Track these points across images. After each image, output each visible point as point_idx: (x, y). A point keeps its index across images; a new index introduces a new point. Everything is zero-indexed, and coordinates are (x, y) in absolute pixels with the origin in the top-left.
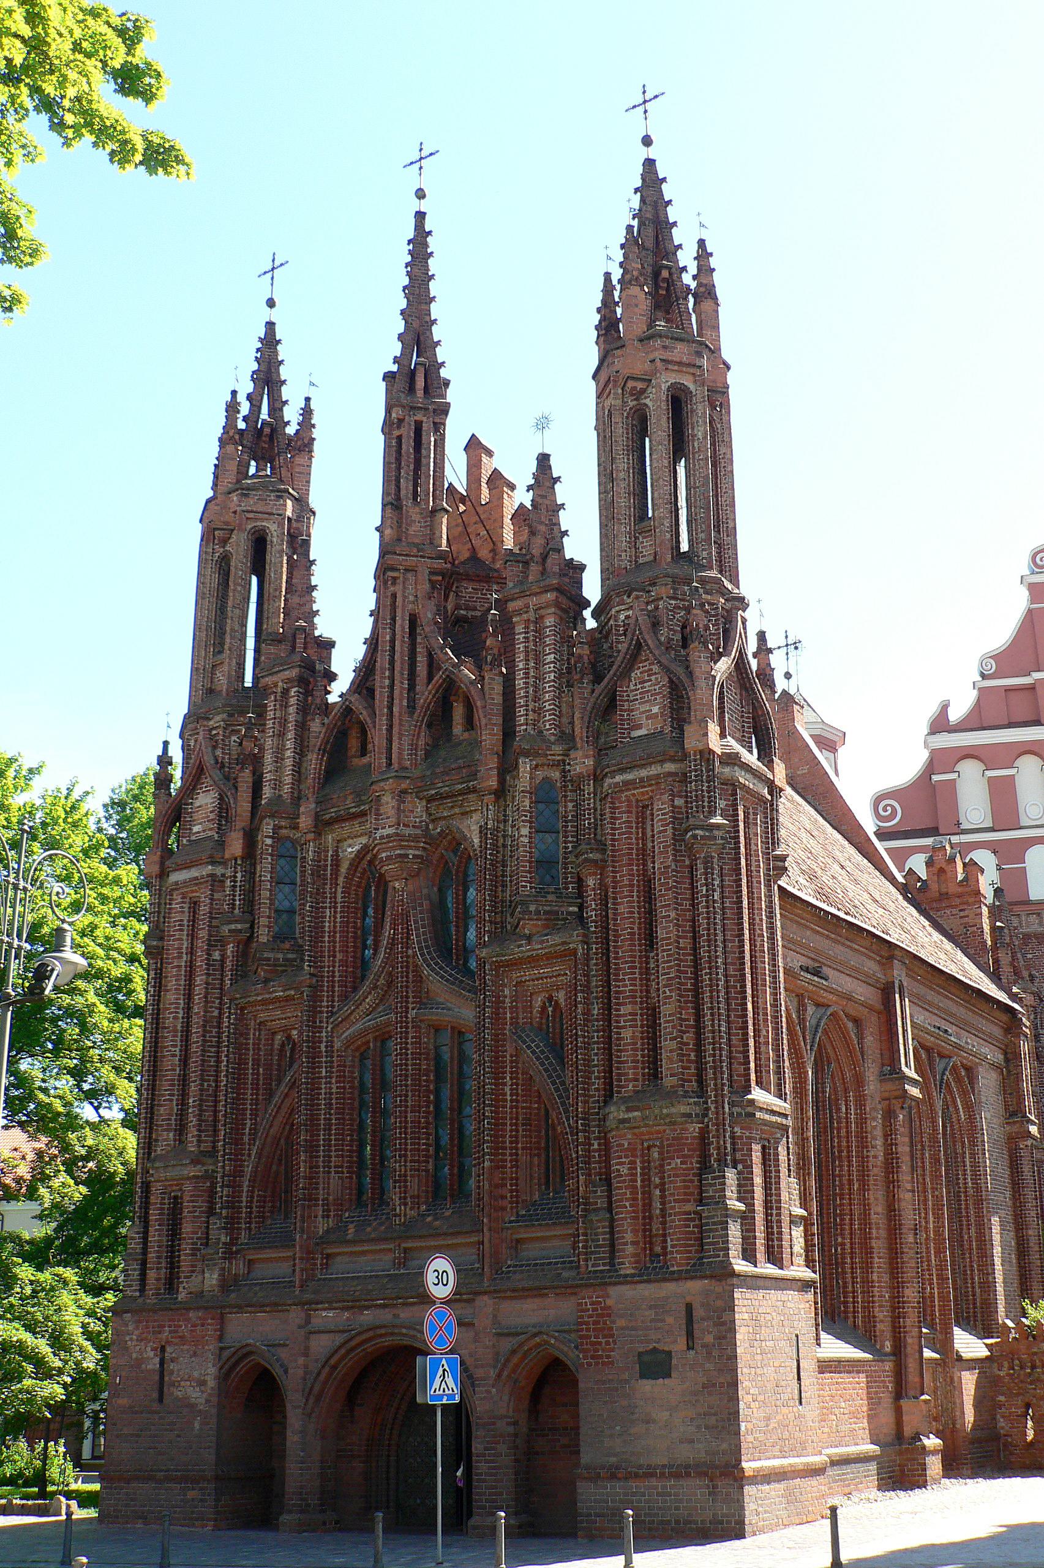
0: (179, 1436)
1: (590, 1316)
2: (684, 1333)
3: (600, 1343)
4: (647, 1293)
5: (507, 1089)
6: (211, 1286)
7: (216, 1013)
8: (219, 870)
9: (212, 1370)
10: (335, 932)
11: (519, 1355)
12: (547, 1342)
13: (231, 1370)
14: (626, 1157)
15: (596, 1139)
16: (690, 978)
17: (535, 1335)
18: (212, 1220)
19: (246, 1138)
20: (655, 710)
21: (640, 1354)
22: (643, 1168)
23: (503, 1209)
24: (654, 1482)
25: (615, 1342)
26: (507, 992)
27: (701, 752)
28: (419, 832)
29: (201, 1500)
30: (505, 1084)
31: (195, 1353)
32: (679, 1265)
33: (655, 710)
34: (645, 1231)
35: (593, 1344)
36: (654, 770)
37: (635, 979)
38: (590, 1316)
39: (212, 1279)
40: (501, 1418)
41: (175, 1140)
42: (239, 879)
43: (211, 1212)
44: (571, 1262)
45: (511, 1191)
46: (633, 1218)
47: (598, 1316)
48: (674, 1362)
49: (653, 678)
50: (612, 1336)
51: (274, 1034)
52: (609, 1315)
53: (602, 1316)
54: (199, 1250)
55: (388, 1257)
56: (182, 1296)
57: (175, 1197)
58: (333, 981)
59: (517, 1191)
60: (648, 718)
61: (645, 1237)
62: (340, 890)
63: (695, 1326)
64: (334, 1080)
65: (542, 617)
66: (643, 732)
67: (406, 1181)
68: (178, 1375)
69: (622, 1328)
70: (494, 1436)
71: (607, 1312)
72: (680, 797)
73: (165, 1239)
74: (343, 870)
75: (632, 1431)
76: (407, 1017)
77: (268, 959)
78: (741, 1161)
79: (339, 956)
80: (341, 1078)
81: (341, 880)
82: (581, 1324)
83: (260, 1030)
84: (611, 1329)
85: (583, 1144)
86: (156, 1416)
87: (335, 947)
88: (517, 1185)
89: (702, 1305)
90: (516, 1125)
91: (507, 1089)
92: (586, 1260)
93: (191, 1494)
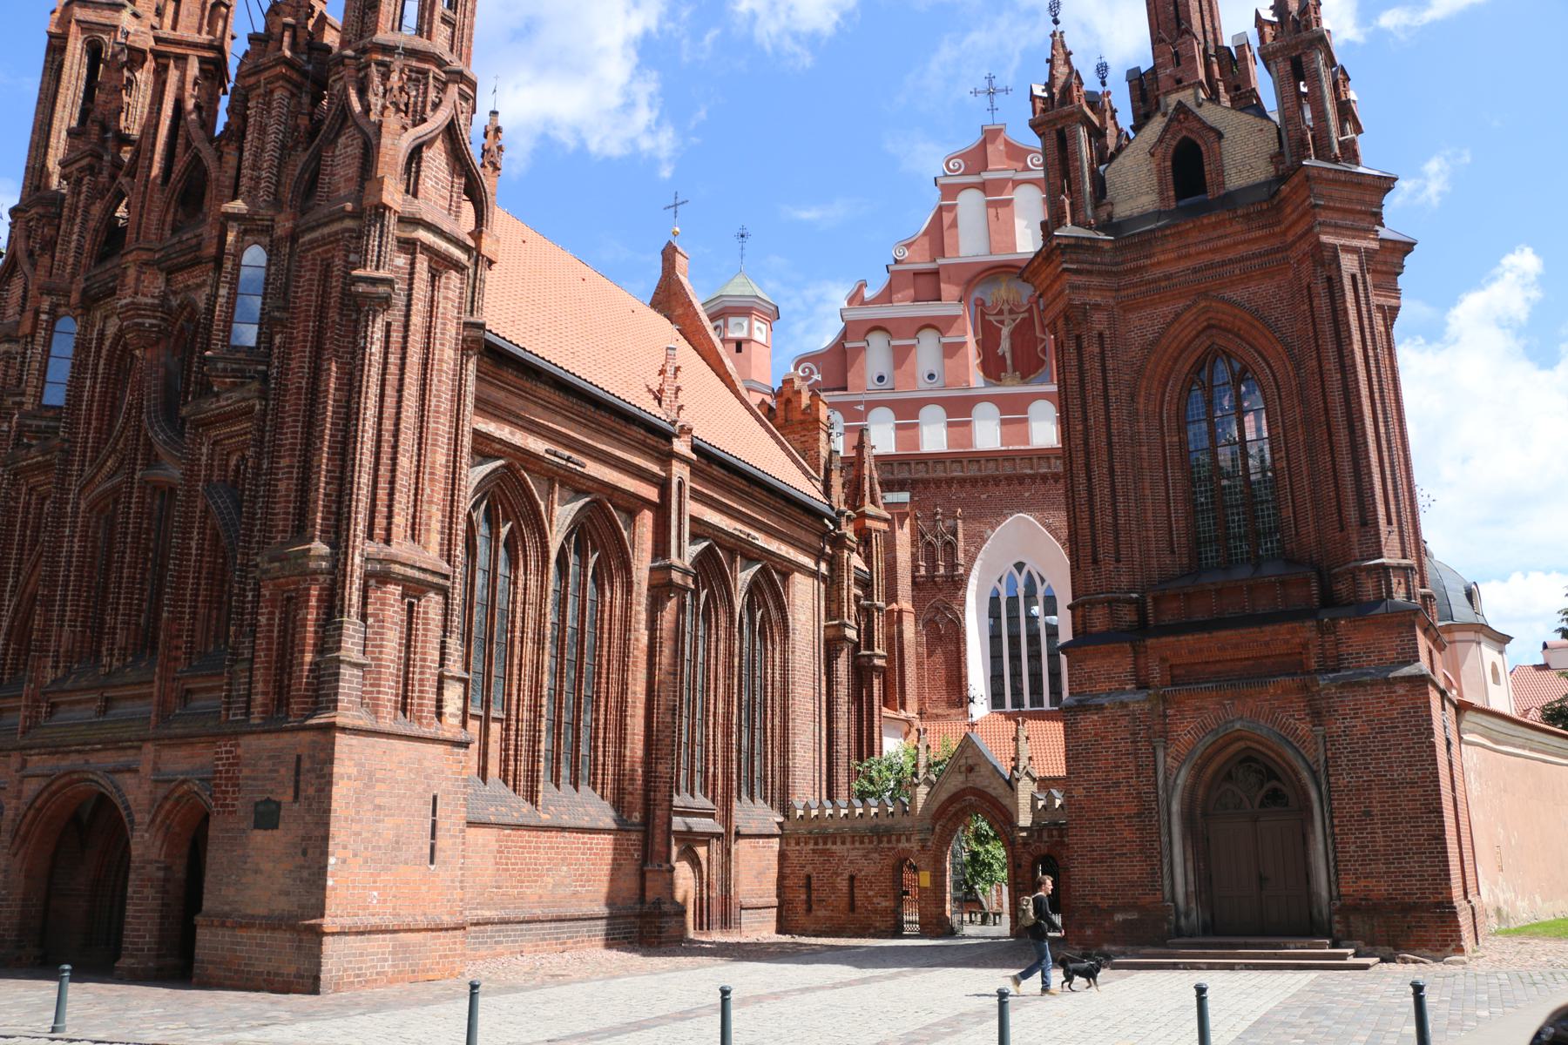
2: (292, 784)
3: (228, 792)
5: (193, 544)
10: (92, 401)
15: (251, 590)
16: (341, 430)
21: (257, 804)
23: (177, 659)
24: (254, 933)
26: (204, 450)
27: (377, 207)
28: (156, 301)
30: (192, 539)
37: (296, 432)
38: (224, 765)
40: (151, 862)
45: (186, 642)
46: (266, 668)
48: (282, 813)
50: (238, 785)
51: (44, 499)
52: (237, 764)
58: (86, 447)
59: (192, 642)
61: (275, 687)
62: (102, 362)
63: (302, 777)
64: (76, 540)
65: (272, 92)
67: (115, 634)
69: (247, 778)
70: (142, 880)
71: (236, 762)
72: (356, 253)
74: (107, 343)
76: (133, 478)
77: (30, 426)
78: (372, 615)
79: (94, 423)
80: (84, 538)
81: (104, 353)
82: (216, 772)
83: (30, 495)
85: (237, 595)
87: (90, 415)
88: (192, 636)
89: (309, 756)
90: (198, 578)
91: (193, 544)
92: (228, 710)
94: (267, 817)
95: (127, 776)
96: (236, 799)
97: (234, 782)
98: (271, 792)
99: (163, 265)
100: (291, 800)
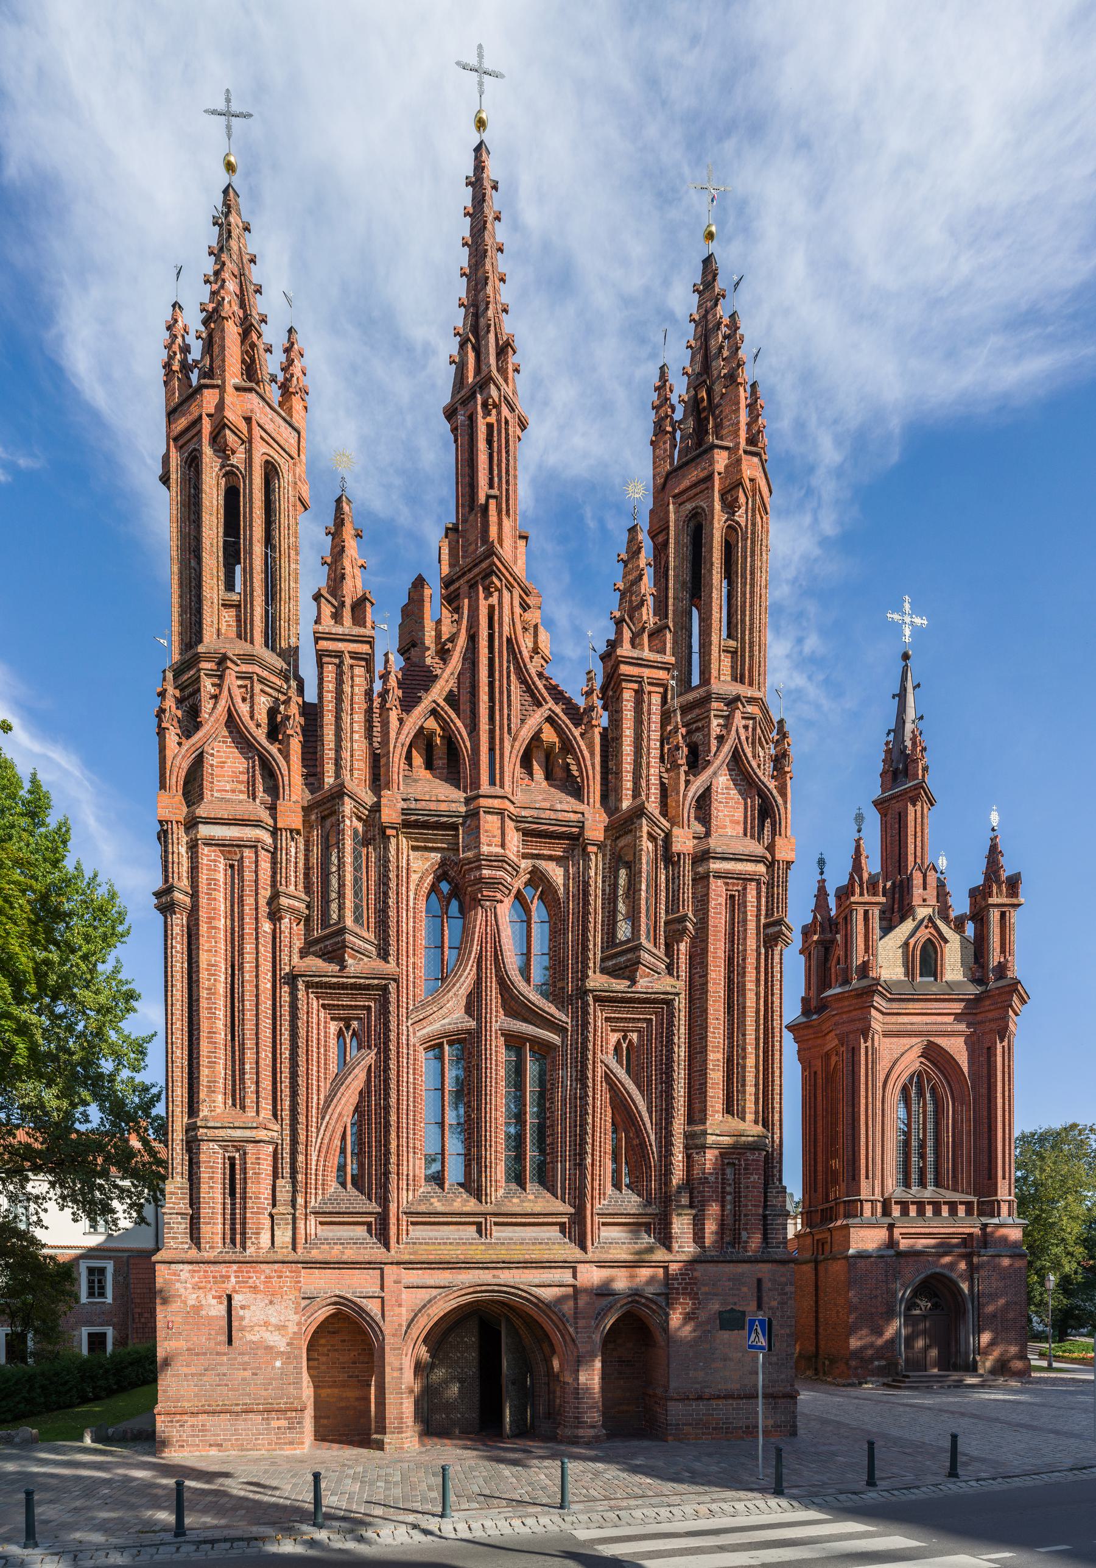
0: (254, 1374)
4: (727, 1270)
12: (637, 1302)
18: (280, 1182)
22: (723, 1179)
29: (289, 1428)
31: (271, 1302)
47: (686, 1284)
52: (695, 1284)
53: (690, 1284)
54: (266, 1209)
56: (251, 1250)
57: (229, 1158)
69: (706, 1294)
84: (697, 1294)
86: (225, 1358)
93: (275, 1424)
98: (735, 1304)
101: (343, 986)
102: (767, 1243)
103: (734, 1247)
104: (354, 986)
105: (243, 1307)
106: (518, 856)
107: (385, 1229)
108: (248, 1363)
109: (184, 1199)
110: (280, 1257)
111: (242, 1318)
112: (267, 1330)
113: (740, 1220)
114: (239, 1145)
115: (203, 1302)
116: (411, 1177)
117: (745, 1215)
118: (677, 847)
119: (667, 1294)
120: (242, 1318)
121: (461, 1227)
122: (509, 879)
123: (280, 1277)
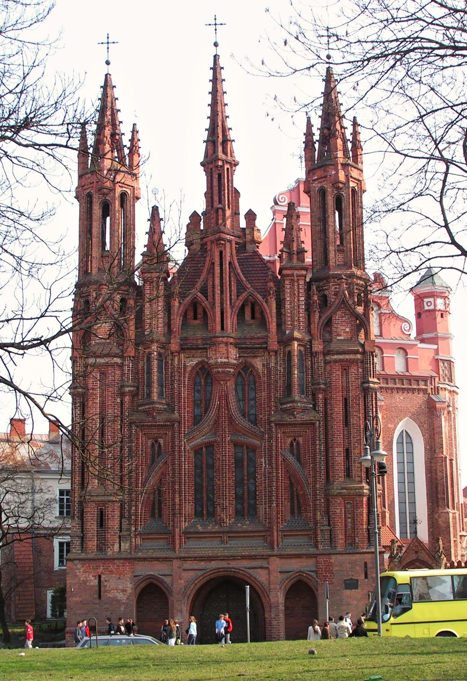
1: (323, 566)
5: (280, 475)
6: (125, 549)
7: (119, 427)
8: (118, 360)
9: (130, 585)
11: (288, 580)
12: (302, 576)
13: (138, 586)
14: (339, 506)
17: (297, 572)
19: (140, 485)
20: (348, 330)
21: (345, 580)
25: (334, 576)
31: (119, 578)
32: (361, 548)
33: (348, 330)
34: (346, 534)
35: (324, 576)
36: (352, 357)
38: (323, 566)
39: (125, 546)
41: (98, 483)
42: (131, 366)
43: (122, 516)
44: (311, 545)
48: (359, 583)
49: (347, 316)
51: (149, 439)
52: (331, 566)
53: (329, 566)
55: (219, 539)
56: (110, 553)
60: (344, 332)
61: (346, 537)
66: (342, 338)
68: (110, 587)
69: (337, 570)
71: (331, 564)
73: (96, 527)
75: (342, 608)
77: (158, 408)
81: (187, 375)
94: (351, 584)
95: (259, 570)
96: (333, 578)
97: (331, 572)
99: (238, 346)
100: (364, 578)
101: (154, 426)
102: (370, 543)
103: (352, 546)
104: (158, 425)
105: (106, 581)
106: (236, 359)
107: (174, 541)
108: (109, 608)
109: (79, 529)
110: (123, 556)
111: (106, 586)
112: (117, 592)
113: (355, 532)
114: (104, 503)
115: (88, 579)
116: (187, 515)
117: (357, 529)
118: (315, 349)
119: (317, 571)
120: (106, 586)
121: (212, 539)
122: (232, 370)
123: (124, 566)
